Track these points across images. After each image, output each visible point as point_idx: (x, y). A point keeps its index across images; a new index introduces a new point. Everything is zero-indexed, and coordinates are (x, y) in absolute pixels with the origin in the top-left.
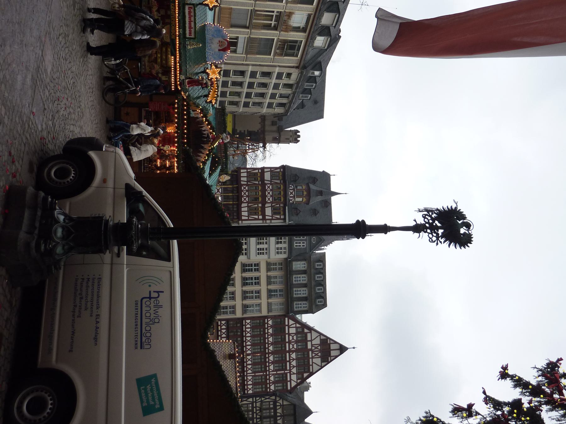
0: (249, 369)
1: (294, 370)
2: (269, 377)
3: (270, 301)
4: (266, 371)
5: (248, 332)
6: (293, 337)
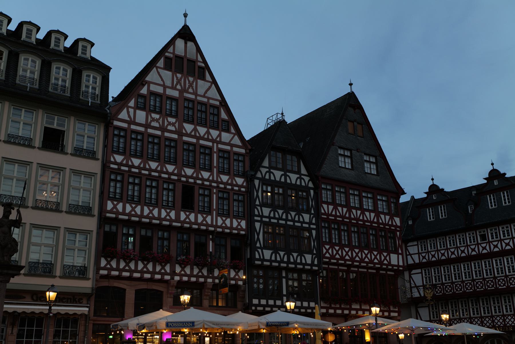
0: (204, 219)
1: (214, 133)
2: (222, 183)
3: (69, 149)
4: (210, 188)
5: (133, 209)
6: (153, 120)
